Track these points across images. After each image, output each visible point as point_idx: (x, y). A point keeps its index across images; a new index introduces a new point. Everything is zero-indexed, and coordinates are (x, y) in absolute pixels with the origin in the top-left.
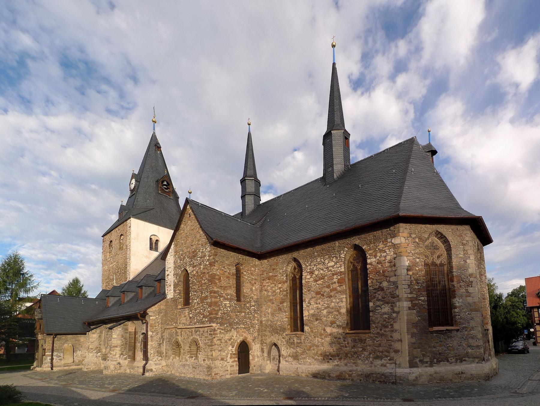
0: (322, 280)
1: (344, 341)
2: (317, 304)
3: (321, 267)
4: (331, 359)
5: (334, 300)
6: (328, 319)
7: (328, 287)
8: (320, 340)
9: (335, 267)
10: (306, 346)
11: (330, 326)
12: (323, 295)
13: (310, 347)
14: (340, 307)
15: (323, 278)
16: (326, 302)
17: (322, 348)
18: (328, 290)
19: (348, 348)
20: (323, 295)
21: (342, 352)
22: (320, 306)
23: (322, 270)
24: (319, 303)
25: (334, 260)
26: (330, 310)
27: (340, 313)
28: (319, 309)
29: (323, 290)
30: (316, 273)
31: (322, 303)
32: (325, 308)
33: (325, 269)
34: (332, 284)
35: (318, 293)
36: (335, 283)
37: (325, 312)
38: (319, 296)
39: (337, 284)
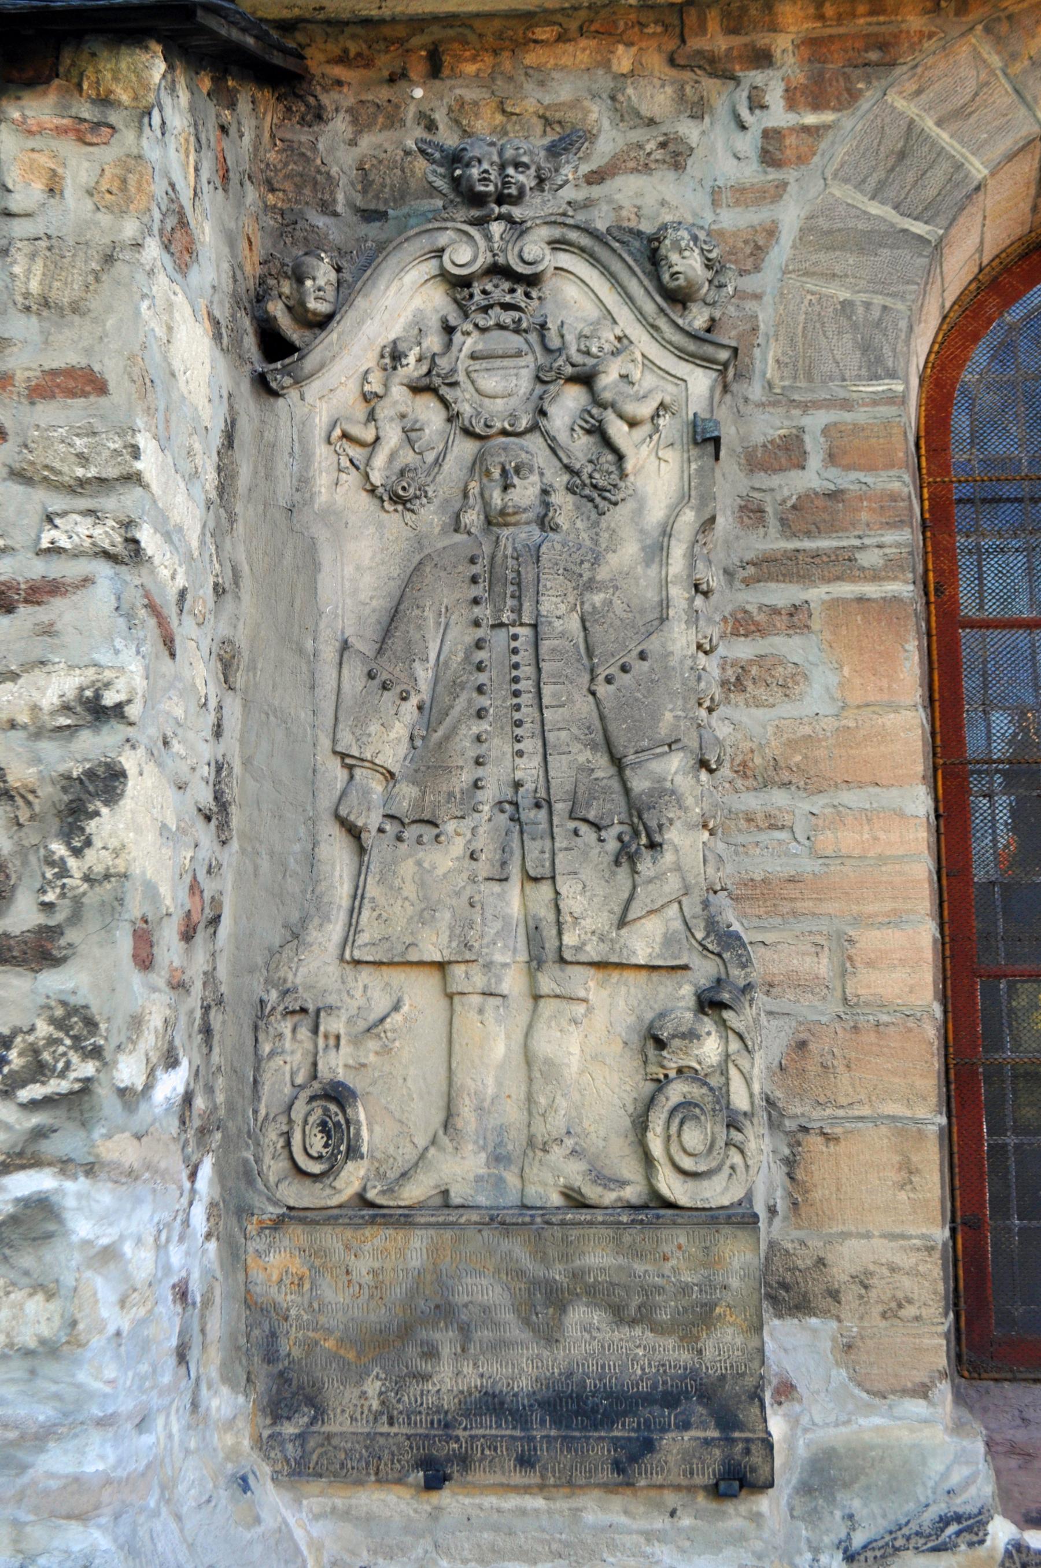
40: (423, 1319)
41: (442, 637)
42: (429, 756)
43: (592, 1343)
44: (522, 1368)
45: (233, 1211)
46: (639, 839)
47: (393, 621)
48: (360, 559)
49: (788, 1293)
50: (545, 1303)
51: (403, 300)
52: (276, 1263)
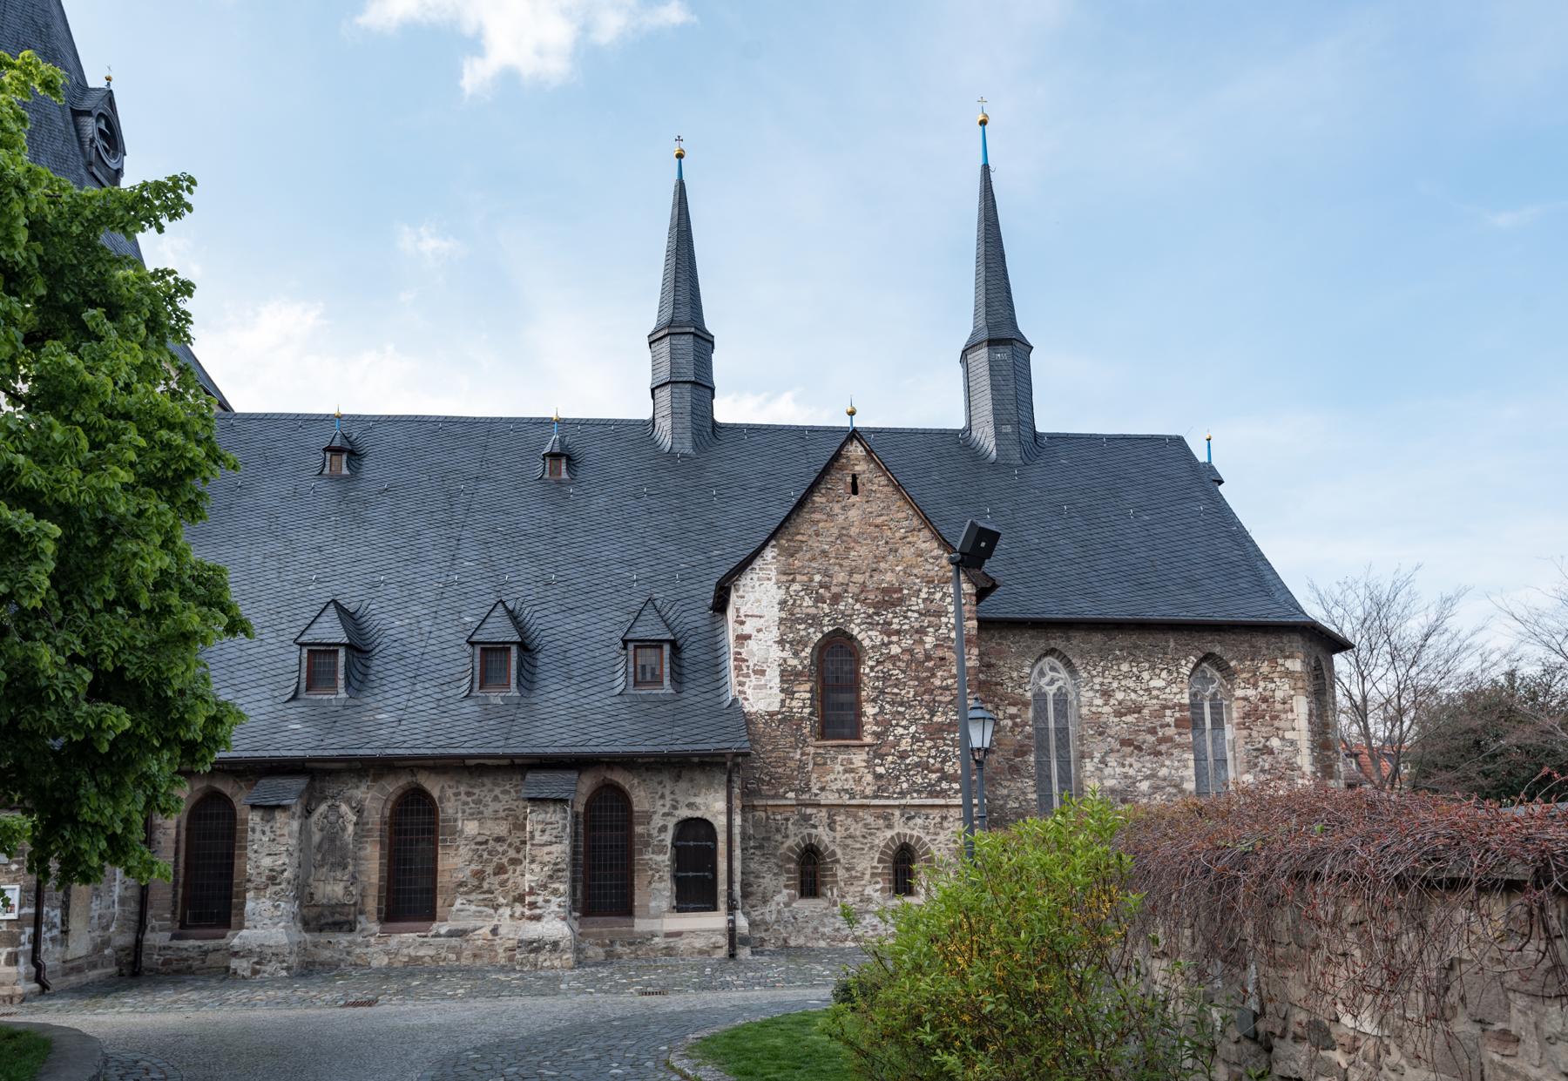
2: (1123, 766)
3: (1132, 685)
5: (1167, 763)
7: (1153, 731)
12: (1139, 748)
18: (1151, 739)
22: (1131, 772)
25: (1164, 674)
27: (1182, 791)
31: (1137, 765)
32: (1147, 778)
34: (1162, 726)
35: (1124, 743)
36: (1168, 725)
37: (1144, 786)
38: (1129, 750)
40: (321, 915)
41: (326, 846)
42: (323, 859)
43: (337, 917)
44: (330, 920)
45: (300, 906)
46: (345, 868)
47: (320, 845)
48: (317, 837)
49: (361, 913)
50: (333, 914)
51: (323, 808)
52: (305, 911)
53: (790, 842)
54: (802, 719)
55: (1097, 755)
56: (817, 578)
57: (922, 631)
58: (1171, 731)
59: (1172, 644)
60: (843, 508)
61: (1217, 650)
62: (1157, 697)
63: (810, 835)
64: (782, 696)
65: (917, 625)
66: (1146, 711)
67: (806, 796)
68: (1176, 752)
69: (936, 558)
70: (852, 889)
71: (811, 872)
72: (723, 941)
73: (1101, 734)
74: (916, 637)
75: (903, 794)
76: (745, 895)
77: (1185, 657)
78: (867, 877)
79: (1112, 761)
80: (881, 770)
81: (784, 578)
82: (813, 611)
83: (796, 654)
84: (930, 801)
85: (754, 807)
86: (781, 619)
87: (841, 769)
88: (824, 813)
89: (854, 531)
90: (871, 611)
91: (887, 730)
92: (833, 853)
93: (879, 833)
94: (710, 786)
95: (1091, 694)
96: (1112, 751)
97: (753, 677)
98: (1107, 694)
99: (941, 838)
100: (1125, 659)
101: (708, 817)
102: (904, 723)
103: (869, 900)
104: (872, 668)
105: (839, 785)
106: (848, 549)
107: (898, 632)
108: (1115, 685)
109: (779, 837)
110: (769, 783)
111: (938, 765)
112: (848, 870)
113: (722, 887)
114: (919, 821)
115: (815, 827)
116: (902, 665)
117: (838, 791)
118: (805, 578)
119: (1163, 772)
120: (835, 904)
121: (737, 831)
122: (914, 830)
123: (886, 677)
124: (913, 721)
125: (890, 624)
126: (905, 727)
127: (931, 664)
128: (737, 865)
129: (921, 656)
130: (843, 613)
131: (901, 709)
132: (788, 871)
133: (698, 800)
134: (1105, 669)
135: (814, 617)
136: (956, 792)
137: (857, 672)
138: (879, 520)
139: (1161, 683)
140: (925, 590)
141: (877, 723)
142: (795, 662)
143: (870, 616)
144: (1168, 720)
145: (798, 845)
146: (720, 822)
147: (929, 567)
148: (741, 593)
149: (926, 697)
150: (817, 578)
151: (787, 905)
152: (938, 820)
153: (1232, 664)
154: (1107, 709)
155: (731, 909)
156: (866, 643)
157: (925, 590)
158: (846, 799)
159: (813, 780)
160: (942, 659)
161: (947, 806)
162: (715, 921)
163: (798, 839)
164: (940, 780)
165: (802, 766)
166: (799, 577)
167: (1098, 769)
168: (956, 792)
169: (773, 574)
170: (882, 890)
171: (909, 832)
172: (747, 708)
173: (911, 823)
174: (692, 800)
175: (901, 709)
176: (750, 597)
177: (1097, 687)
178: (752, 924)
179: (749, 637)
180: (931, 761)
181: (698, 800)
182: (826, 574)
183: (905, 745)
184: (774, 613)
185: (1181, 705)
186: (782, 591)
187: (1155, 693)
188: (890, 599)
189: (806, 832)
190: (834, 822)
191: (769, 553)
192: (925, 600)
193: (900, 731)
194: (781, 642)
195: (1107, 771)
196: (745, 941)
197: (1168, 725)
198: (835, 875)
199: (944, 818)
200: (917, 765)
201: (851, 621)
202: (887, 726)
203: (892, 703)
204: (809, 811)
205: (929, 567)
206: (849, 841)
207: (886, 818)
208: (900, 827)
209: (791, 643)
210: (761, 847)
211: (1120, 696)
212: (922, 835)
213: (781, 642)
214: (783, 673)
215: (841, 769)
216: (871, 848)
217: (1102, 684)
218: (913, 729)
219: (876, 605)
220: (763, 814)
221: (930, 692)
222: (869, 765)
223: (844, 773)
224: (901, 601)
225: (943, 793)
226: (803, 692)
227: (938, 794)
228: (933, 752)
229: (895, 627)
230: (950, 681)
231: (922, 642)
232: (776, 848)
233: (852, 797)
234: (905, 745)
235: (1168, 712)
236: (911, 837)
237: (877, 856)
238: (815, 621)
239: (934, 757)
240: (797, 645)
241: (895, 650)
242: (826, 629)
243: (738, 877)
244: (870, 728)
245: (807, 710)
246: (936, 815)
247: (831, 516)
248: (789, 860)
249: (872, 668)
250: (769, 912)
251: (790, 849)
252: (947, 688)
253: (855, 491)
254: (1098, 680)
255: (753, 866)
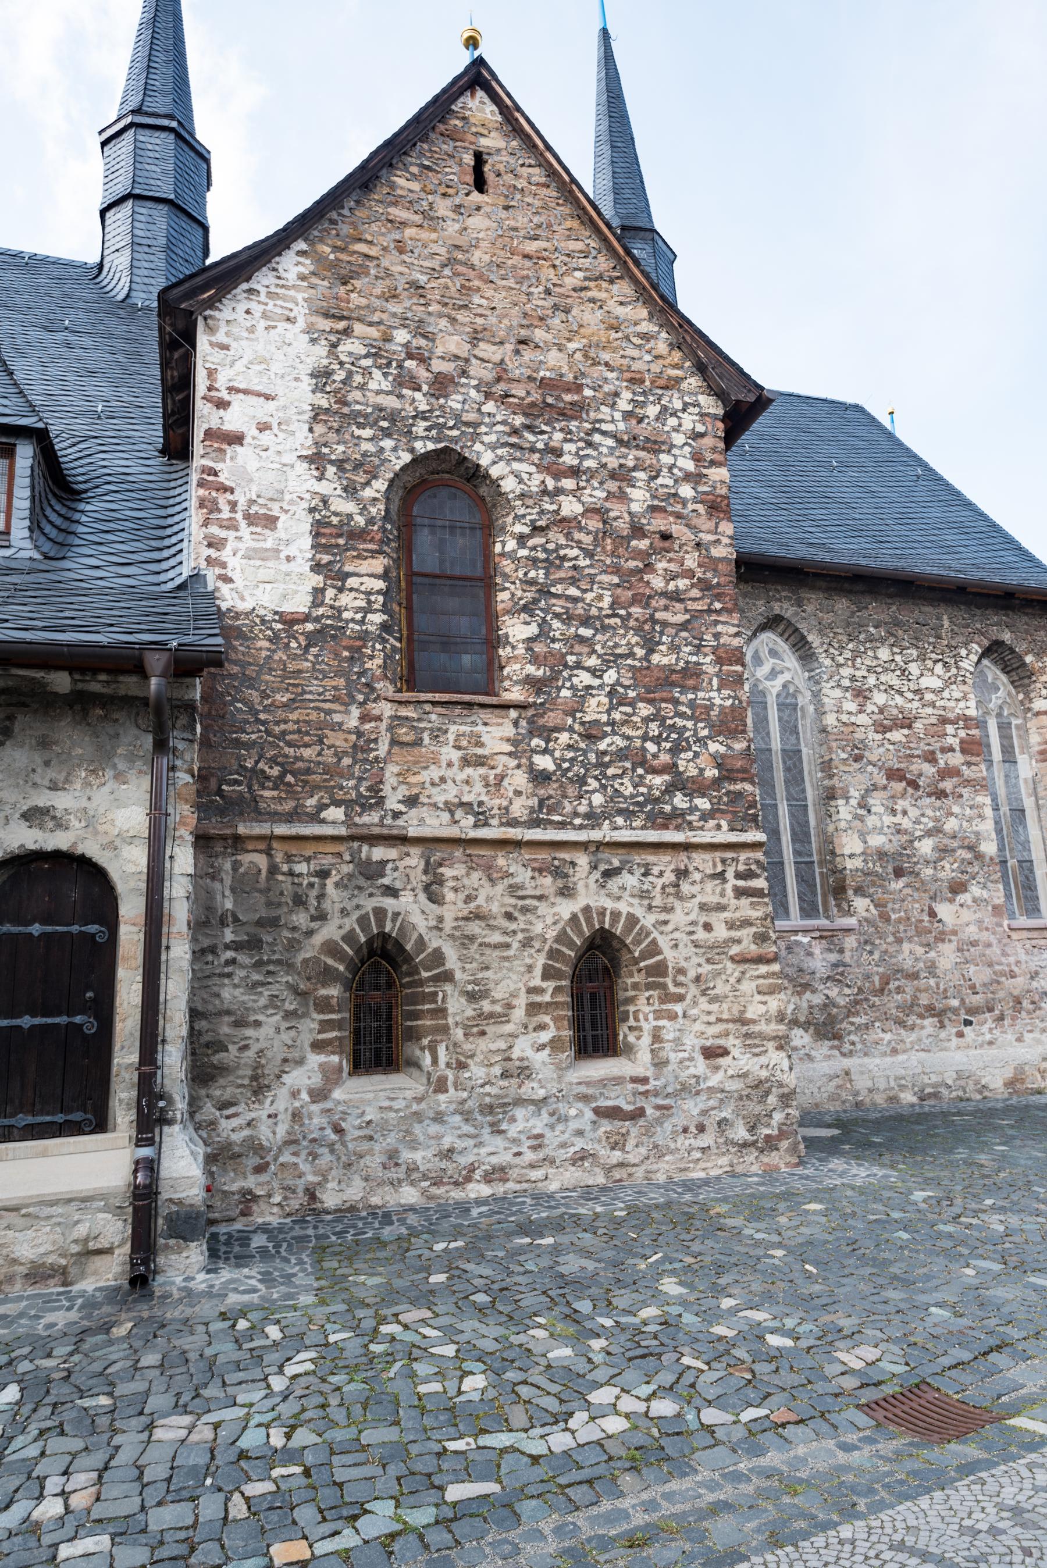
0: (906, 731)
1: (1004, 954)
2: (894, 812)
3: (895, 682)
4: (968, 1023)
6: (942, 875)
7: (930, 758)
8: (920, 950)
9: (946, 694)
10: (868, 977)
11: (951, 901)
12: (914, 784)
13: (886, 981)
14: (977, 834)
15: (907, 723)
16: (929, 812)
17: (932, 982)
18: (929, 769)
19: (1020, 980)
20: (914, 784)
21: (1001, 994)
22: (906, 823)
23: (900, 693)
24: (905, 813)
25: (939, 668)
26: (947, 841)
27: (979, 856)
28: (906, 832)
29: (913, 767)
30: (880, 698)
31: (913, 813)
32: (929, 833)
33: (910, 696)
34: (943, 750)
35: (896, 775)
36: (952, 750)
37: (926, 847)
38: (899, 786)
39: (958, 754)
53: (331, 931)
54: (364, 636)
55: (855, 794)
56: (401, 336)
57: (621, 475)
58: (956, 759)
59: (946, 623)
60: (458, 209)
61: (1007, 637)
62: (933, 704)
63: (380, 913)
64: (318, 580)
65: (613, 463)
66: (918, 725)
67: (372, 818)
68: (965, 792)
69: (646, 337)
70: (483, 1045)
71: (381, 1006)
72: (114, 1230)
73: (858, 759)
74: (612, 486)
75: (593, 818)
76: (202, 1074)
77: (966, 644)
78: (519, 1014)
79: (876, 801)
80: (544, 762)
81: (326, 324)
82: (391, 402)
83: (351, 491)
84: (652, 836)
85: (238, 842)
86: (318, 414)
87: (456, 755)
88: (415, 859)
89: (478, 257)
90: (519, 420)
91: (555, 676)
92: (438, 957)
93: (543, 908)
94: (101, 761)
95: (838, 693)
96: (875, 787)
97: (245, 530)
98: (861, 694)
99: (678, 918)
100: (883, 641)
101: (91, 849)
102: (592, 662)
103: (524, 1072)
104: (522, 539)
105: (450, 793)
106: (466, 290)
107: (575, 472)
108: (872, 680)
109: (301, 919)
110: (279, 782)
111: (665, 758)
112: (472, 997)
113: (125, 1056)
114: (630, 880)
115: (392, 892)
116: (587, 540)
117: (450, 808)
118: (374, 332)
119: (951, 825)
120: (441, 1086)
121: (178, 891)
122: (619, 900)
123: (553, 561)
124: (612, 659)
125: (558, 453)
126: (593, 672)
127: (643, 544)
128: (176, 991)
129: (622, 526)
130: (457, 417)
131: (586, 632)
132: (323, 1006)
133: (61, 801)
134: (856, 654)
135: (393, 417)
136: (705, 817)
137: (487, 554)
138: (531, 247)
139: (937, 683)
140: (627, 395)
141: (535, 659)
142: (349, 507)
143: (515, 432)
144: (950, 740)
145: (349, 938)
146: (127, 868)
147: (631, 352)
148: (220, 337)
149: (636, 610)
150: (401, 336)
151: (319, 1095)
152: (670, 877)
153: (1029, 659)
154: (862, 719)
155: (150, 1122)
156: (509, 485)
157: (627, 395)
158: (466, 827)
159: (390, 779)
160: (666, 537)
161: (687, 847)
162: (93, 1165)
163: (351, 923)
164: (670, 790)
165: (362, 745)
166: (359, 328)
167: (857, 817)
168: (705, 817)
169: (300, 312)
170: (555, 1045)
171: (609, 904)
172: (228, 599)
173: (614, 884)
174: (43, 799)
175: (586, 632)
176: (244, 349)
177: (846, 683)
178: (219, 1157)
179: (237, 439)
180: (651, 747)
181: (61, 801)
182: (420, 329)
183: (595, 709)
184: (302, 395)
185: (967, 719)
186: (321, 350)
187: (929, 697)
188: (555, 403)
189: (369, 905)
190: (440, 881)
191: (292, 265)
192: (627, 415)
193: (584, 678)
194: (317, 460)
195: (871, 821)
196: (188, 1225)
197: (952, 750)
198: (442, 1012)
199: (682, 874)
200: (622, 755)
201: (476, 437)
202: (558, 665)
203: (567, 618)
204: (378, 853)
205: (631, 352)
206: (475, 928)
207: (558, 873)
208: (588, 894)
209: (340, 464)
210: (253, 944)
211: (880, 698)
212: (639, 912)
213: (317, 460)
214: (319, 529)
215: (456, 755)
216: (526, 943)
217: (853, 679)
218: (611, 676)
219: (529, 410)
220: (261, 861)
221: (643, 600)
222: (518, 749)
223: (459, 769)
224: (577, 410)
225: (676, 819)
226: (368, 574)
227: (666, 821)
228: (654, 729)
229: (568, 460)
230: (682, 583)
231: (622, 497)
232: (293, 946)
233: (482, 819)
234: (595, 709)
235: (950, 729)
236: (616, 915)
237: (541, 960)
238: (394, 424)
239: (657, 740)
240: (355, 470)
241: (570, 507)
242: (420, 446)
243: (175, 1024)
244: (517, 669)
245: (377, 618)
246: (665, 864)
247: (430, 219)
248: (327, 975)
249: (522, 539)
250: (266, 1120)
251: (331, 948)
252: (676, 597)
253: (480, 184)
254: (846, 672)
255: (230, 994)
